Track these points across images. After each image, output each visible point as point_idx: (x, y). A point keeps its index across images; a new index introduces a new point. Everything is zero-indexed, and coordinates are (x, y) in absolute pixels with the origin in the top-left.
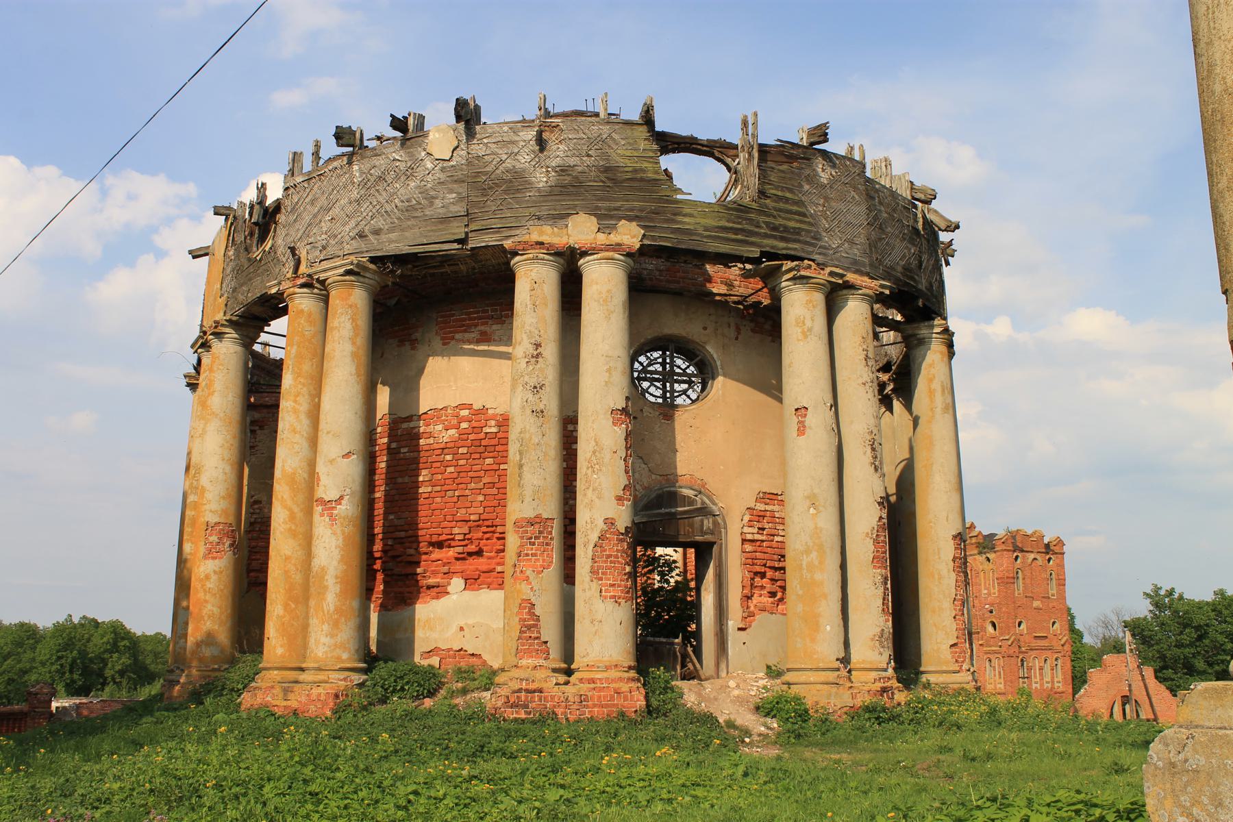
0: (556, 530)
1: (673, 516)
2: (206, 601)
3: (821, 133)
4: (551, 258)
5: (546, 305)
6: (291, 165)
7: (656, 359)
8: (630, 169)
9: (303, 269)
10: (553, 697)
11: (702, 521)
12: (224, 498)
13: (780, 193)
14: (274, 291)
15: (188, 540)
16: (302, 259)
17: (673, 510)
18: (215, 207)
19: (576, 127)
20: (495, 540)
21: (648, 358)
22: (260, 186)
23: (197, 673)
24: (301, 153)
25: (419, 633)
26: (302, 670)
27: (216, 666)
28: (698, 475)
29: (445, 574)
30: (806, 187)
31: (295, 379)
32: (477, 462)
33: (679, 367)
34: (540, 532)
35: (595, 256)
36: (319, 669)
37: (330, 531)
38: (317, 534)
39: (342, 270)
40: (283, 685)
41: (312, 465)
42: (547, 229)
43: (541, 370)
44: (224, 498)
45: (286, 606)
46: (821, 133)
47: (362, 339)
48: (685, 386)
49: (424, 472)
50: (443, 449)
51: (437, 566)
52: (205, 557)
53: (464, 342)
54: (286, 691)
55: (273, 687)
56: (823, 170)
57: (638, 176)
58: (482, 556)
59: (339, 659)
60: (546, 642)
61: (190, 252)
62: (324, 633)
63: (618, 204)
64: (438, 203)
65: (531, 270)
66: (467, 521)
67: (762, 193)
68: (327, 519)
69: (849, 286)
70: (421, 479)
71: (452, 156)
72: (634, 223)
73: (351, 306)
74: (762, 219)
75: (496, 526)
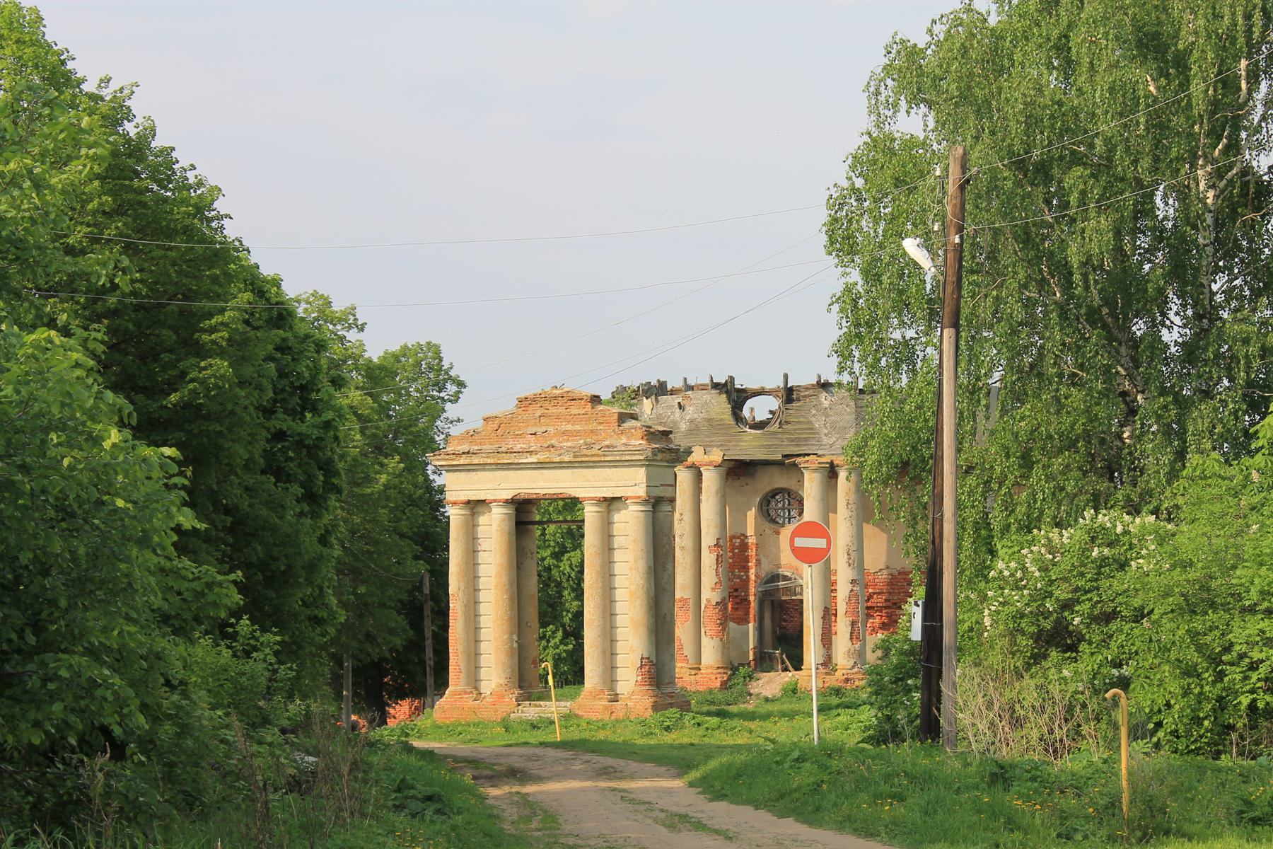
30: (814, 412)
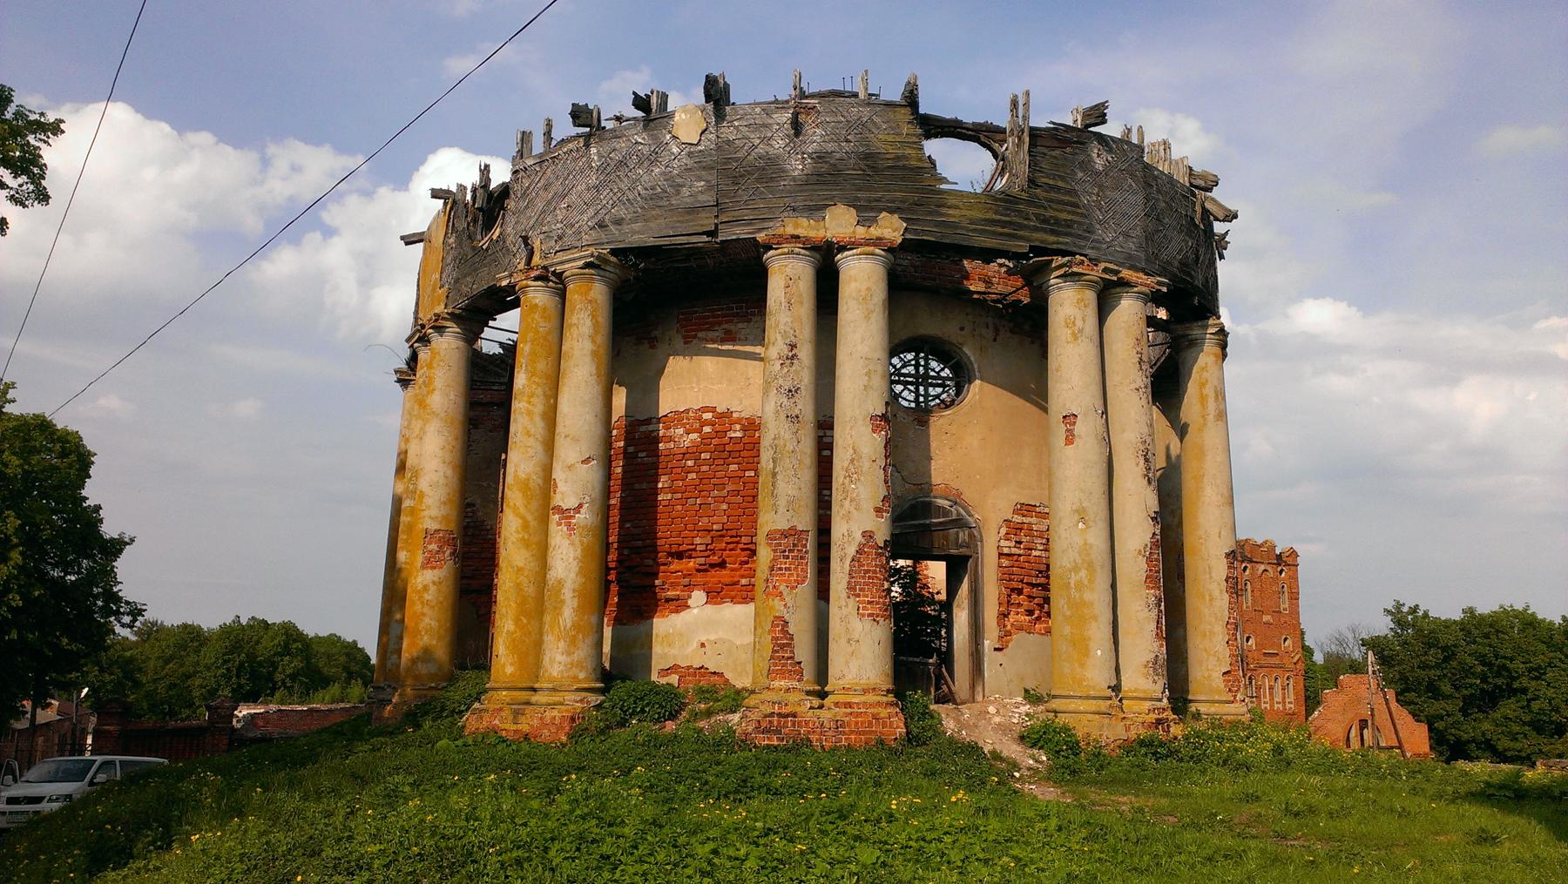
0: (810, 545)
1: (927, 529)
2: (423, 614)
3: (1098, 114)
4: (807, 253)
5: (802, 303)
6: (520, 145)
7: (909, 361)
8: (892, 156)
9: (536, 260)
10: (807, 723)
11: (957, 533)
12: (444, 503)
13: (1051, 182)
14: (504, 283)
15: (402, 548)
16: (535, 249)
17: (928, 522)
18: (433, 190)
19: (834, 109)
20: (739, 551)
21: (901, 360)
22: (483, 168)
23: (412, 692)
24: (530, 132)
25: (657, 649)
26: (535, 690)
27: (433, 685)
28: (954, 485)
29: (685, 586)
30: (1080, 175)
31: (529, 379)
32: (720, 468)
33: (933, 370)
34: (794, 545)
35: (855, 251)
36: (554, 690)
37: (568, 542)
38: (553, 544)
39: (581, 263)
40: (513, 707)
41: (547, 470)
42: (804, 221)
43: (796, 372)
44: (444, 503)
45: (517, 621)
46: (1098, 114)
47: (603, 338)
48: (939, 390)
49: (663, 478)
50: (684, 454)
51: (677, 577)
52: (424, 567)
53: (707, 341)
54: (517, 714)
55: (501, 709)
56: (1098, 157)
57: (900, 164)
58: (725, 568)
59: (575, 678)
60: (800, 663)
61: (402, 238)
62: (560, 650)
63: (879, 194)
64: (685, 191)
65: (786, 266)
66: (709, 531)
67: (1032, 182)
68: (565, 529)
69: (1125, 284)
70: (660, 485)
71: (700, 140)
72: (896, 216)
73: (590, 301)
74: (1031, 210)
75: (741, 537)
